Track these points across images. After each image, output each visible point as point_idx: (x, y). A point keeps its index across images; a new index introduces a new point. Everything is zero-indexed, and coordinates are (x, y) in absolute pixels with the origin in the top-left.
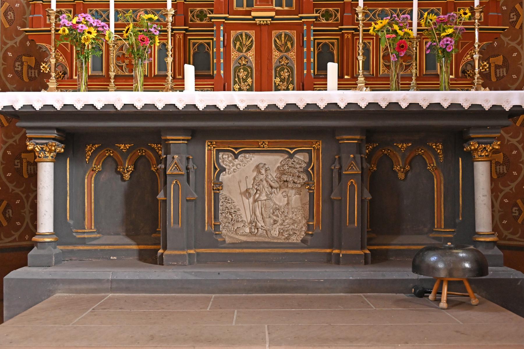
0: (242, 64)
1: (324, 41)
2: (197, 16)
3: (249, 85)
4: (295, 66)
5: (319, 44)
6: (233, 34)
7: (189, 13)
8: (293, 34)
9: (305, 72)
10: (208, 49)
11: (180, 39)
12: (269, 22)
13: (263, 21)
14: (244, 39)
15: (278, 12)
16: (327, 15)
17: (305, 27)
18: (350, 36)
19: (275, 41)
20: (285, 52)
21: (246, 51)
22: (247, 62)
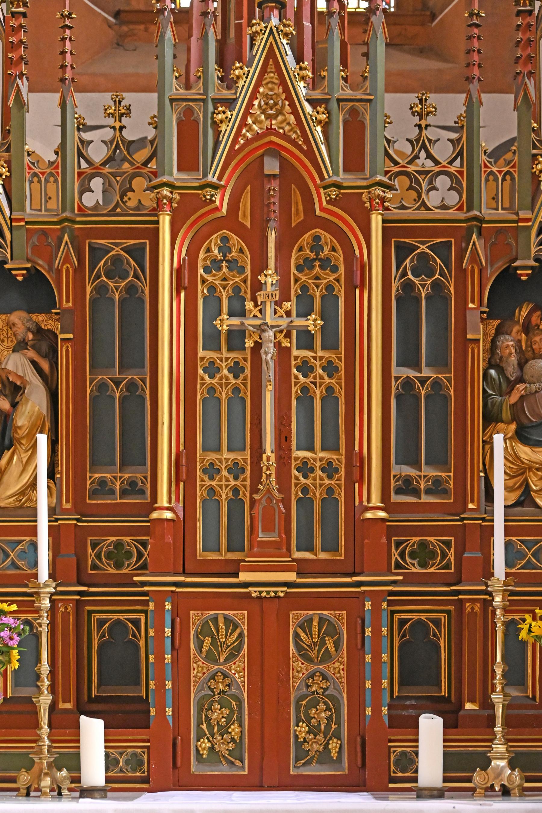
0: (217, 691)
1: (415, 616)
2: (109, 556)
3: (233, 740)
4: (345, 696)
5: (403, 622)
6: (196, 618)
7: (90, 550)
8: (340, 619)
9: (369, 711)
10: (134, 635)
11: (66, 614)
12: (282, 595)
13: (268, 592)
14: (222, 631)
15: (302, 567)
16: (424, 554)
17: (368, 605)
18: (477, 607)
19: (297, 635)
20: (322, 662)
21: (227, 660)
22: (229, 685)
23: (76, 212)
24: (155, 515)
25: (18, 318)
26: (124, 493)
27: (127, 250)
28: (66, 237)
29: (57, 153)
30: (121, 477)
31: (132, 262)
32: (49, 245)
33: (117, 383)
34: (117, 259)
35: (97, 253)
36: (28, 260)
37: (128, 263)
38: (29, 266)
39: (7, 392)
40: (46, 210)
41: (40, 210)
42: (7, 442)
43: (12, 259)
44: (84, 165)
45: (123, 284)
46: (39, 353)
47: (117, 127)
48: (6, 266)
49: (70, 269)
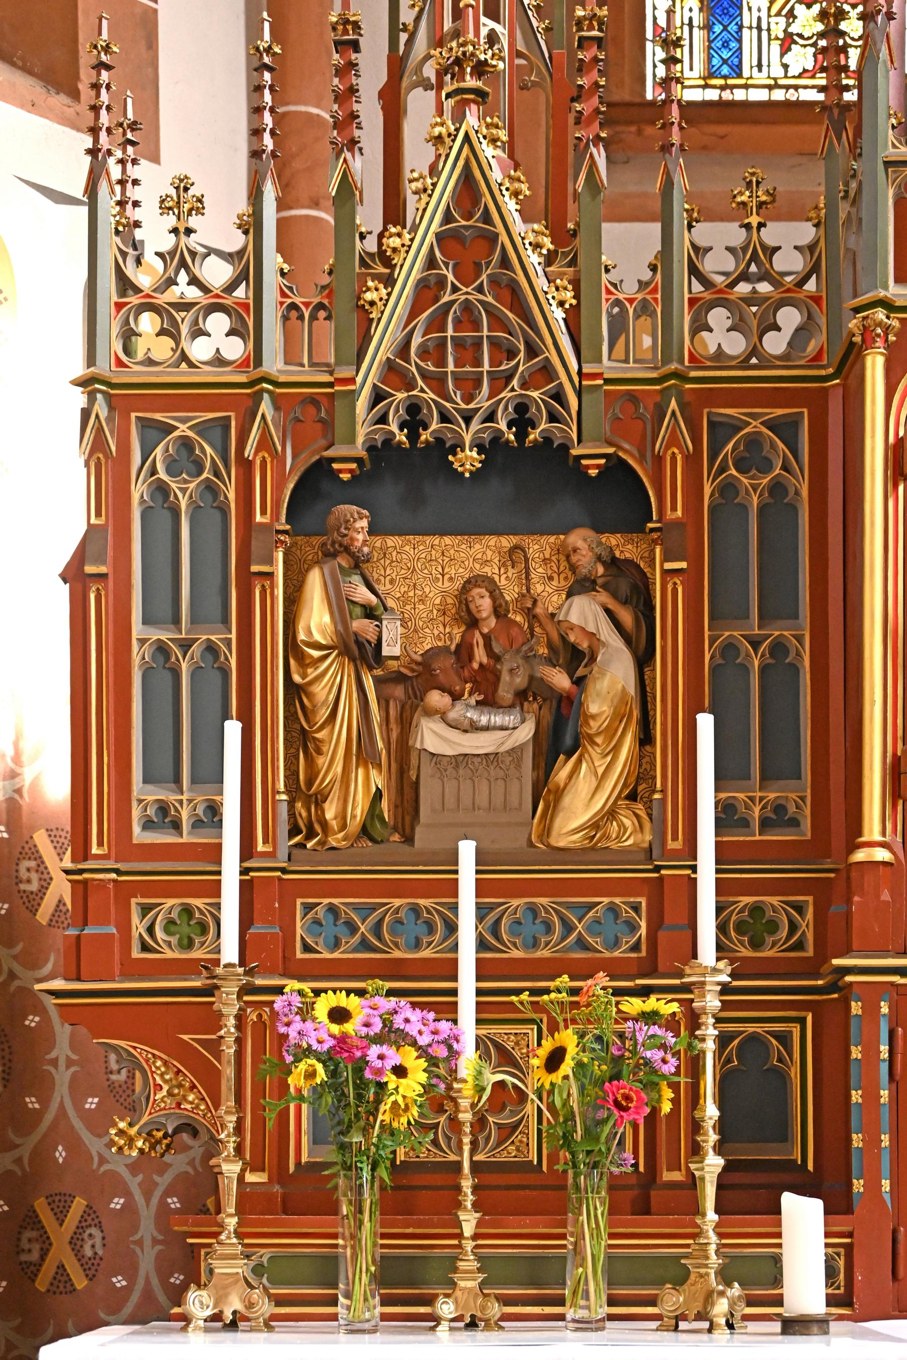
2: (740, 928)
23: (687, 363)
24: (860, 856)
25: (581, 540)
26: (766, 824)
27: (771, 425)
28: (673, 404)
29: (653, 268)
30: (761, 799)
31: (781, 445)
32: (641, 418)
33: (755, 644)
34: (753, 441)
35: (721, 430)
36: (610, 444)
37: (773, 446)
38: (611, 450)
39: (561, 661)
40: (635, 361)
41: (626, 361)
42: (568, 740)
43: (579, 441)
44: (697, 287)
45: (765, 481)
46: (615, 596)
47: (755, 225)
48: (574, 452)
49: (679, 457)
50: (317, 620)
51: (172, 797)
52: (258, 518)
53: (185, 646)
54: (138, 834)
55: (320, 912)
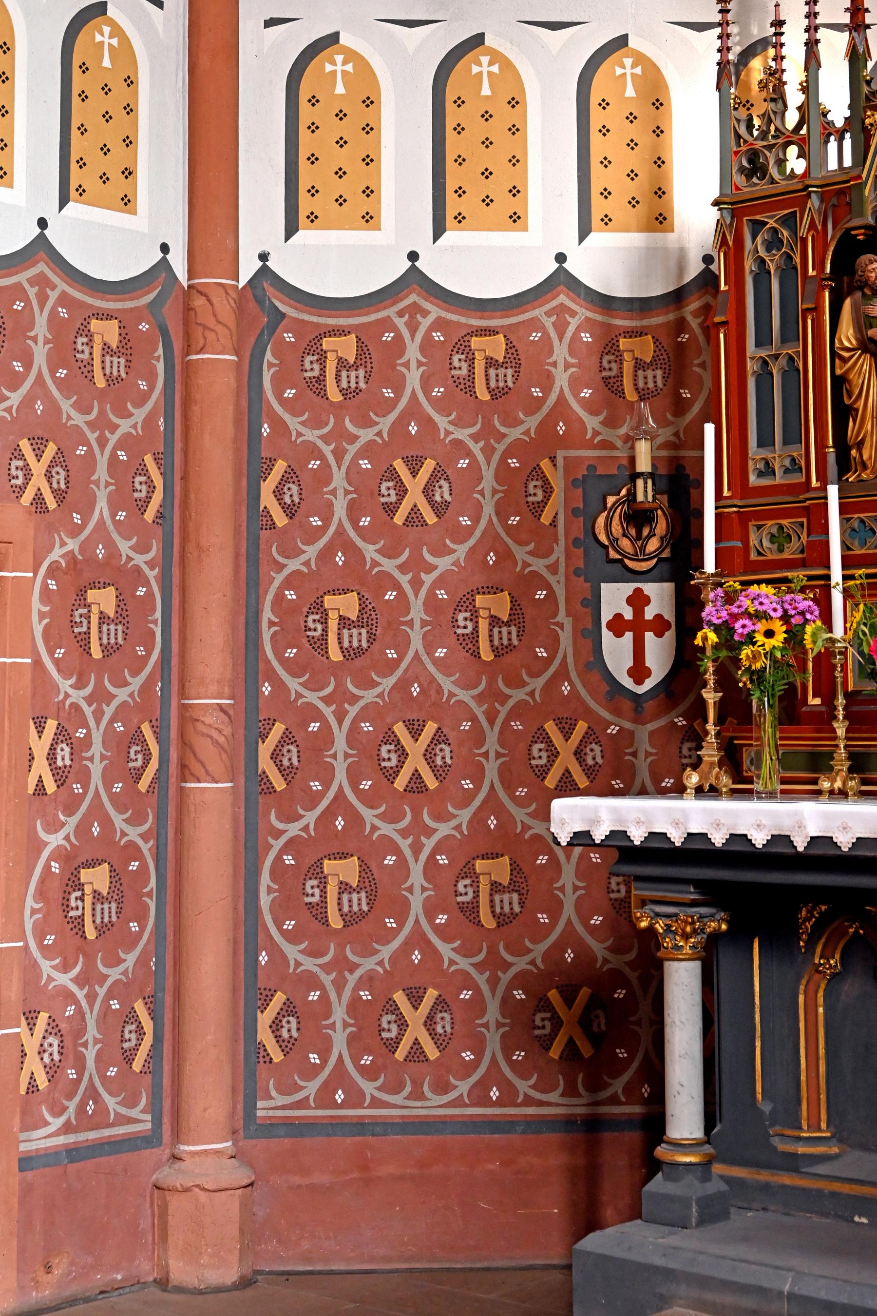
50: (847, 335)
51: (770, 455)
52: (811, 272)
53: (776, 357)
54: (753, 479)
55: (856, 524)
